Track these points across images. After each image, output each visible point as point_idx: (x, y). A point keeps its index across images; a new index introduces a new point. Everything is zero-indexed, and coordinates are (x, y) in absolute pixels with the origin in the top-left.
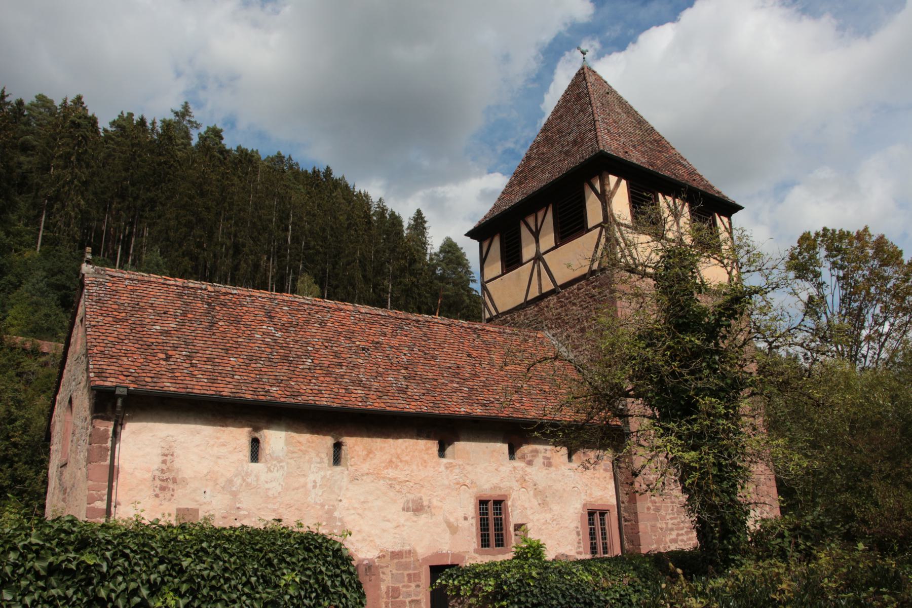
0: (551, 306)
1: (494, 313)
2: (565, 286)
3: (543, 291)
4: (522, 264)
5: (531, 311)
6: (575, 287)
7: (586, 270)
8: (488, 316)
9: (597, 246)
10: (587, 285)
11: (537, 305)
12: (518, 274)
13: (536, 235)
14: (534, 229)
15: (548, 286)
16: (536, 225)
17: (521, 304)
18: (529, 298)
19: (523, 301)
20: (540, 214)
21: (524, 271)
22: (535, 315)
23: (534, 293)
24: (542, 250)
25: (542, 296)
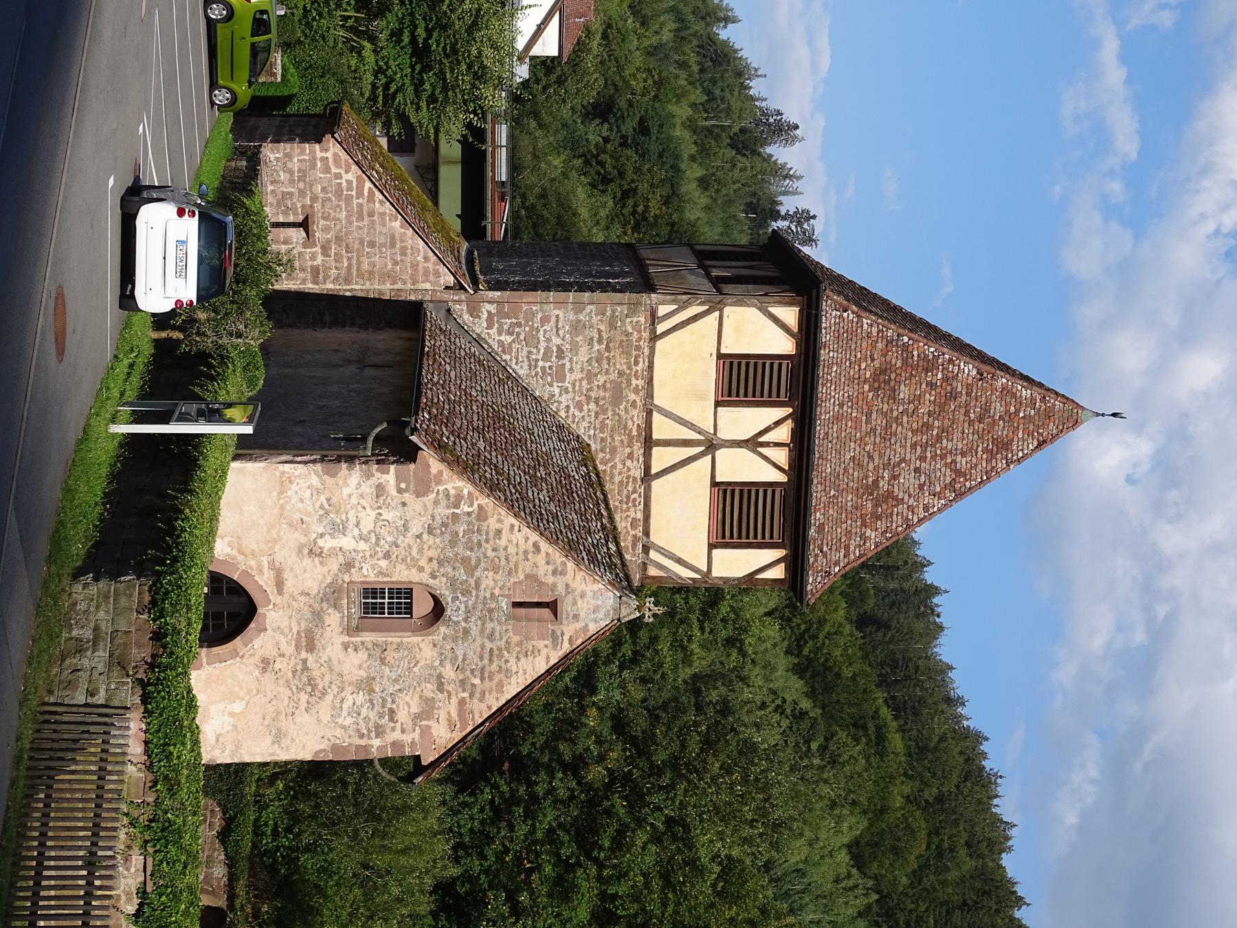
0: (628, 463)
1: (660, 328)
2: (648, 491)
3: (655, 450)
4: (718, 404)
5: (636, 418)
6: (640, 515)
7: (653, 538)
8: (663, 310)
9: (680, 561)
10: (635, 536)
11: (639, 435)
12: (702, 397)
13: (753, 444)
14: (760, 440)
15: (662, 458)
16: (767, 444)
17: (652, 397)
18: (656, 417)
19: (656, 402)
20: (781, 456)
21: (701, 412)
22: (625, 427)
23: (662, 428)
24: (720, 454)
25: (649, 443)
